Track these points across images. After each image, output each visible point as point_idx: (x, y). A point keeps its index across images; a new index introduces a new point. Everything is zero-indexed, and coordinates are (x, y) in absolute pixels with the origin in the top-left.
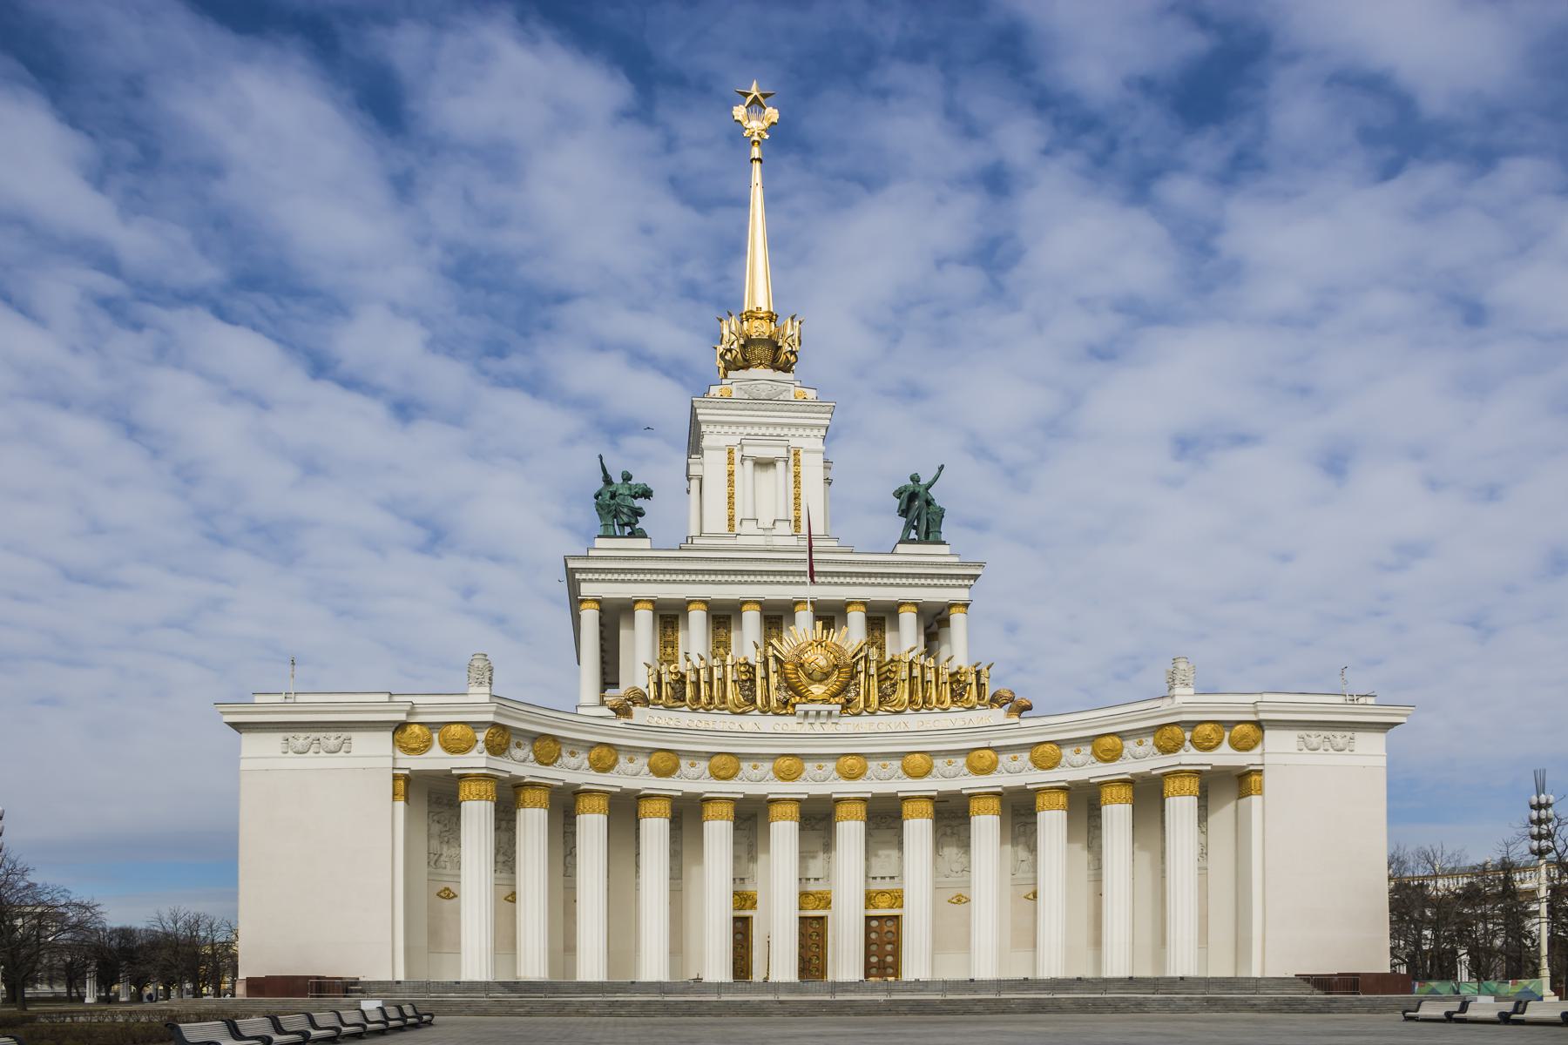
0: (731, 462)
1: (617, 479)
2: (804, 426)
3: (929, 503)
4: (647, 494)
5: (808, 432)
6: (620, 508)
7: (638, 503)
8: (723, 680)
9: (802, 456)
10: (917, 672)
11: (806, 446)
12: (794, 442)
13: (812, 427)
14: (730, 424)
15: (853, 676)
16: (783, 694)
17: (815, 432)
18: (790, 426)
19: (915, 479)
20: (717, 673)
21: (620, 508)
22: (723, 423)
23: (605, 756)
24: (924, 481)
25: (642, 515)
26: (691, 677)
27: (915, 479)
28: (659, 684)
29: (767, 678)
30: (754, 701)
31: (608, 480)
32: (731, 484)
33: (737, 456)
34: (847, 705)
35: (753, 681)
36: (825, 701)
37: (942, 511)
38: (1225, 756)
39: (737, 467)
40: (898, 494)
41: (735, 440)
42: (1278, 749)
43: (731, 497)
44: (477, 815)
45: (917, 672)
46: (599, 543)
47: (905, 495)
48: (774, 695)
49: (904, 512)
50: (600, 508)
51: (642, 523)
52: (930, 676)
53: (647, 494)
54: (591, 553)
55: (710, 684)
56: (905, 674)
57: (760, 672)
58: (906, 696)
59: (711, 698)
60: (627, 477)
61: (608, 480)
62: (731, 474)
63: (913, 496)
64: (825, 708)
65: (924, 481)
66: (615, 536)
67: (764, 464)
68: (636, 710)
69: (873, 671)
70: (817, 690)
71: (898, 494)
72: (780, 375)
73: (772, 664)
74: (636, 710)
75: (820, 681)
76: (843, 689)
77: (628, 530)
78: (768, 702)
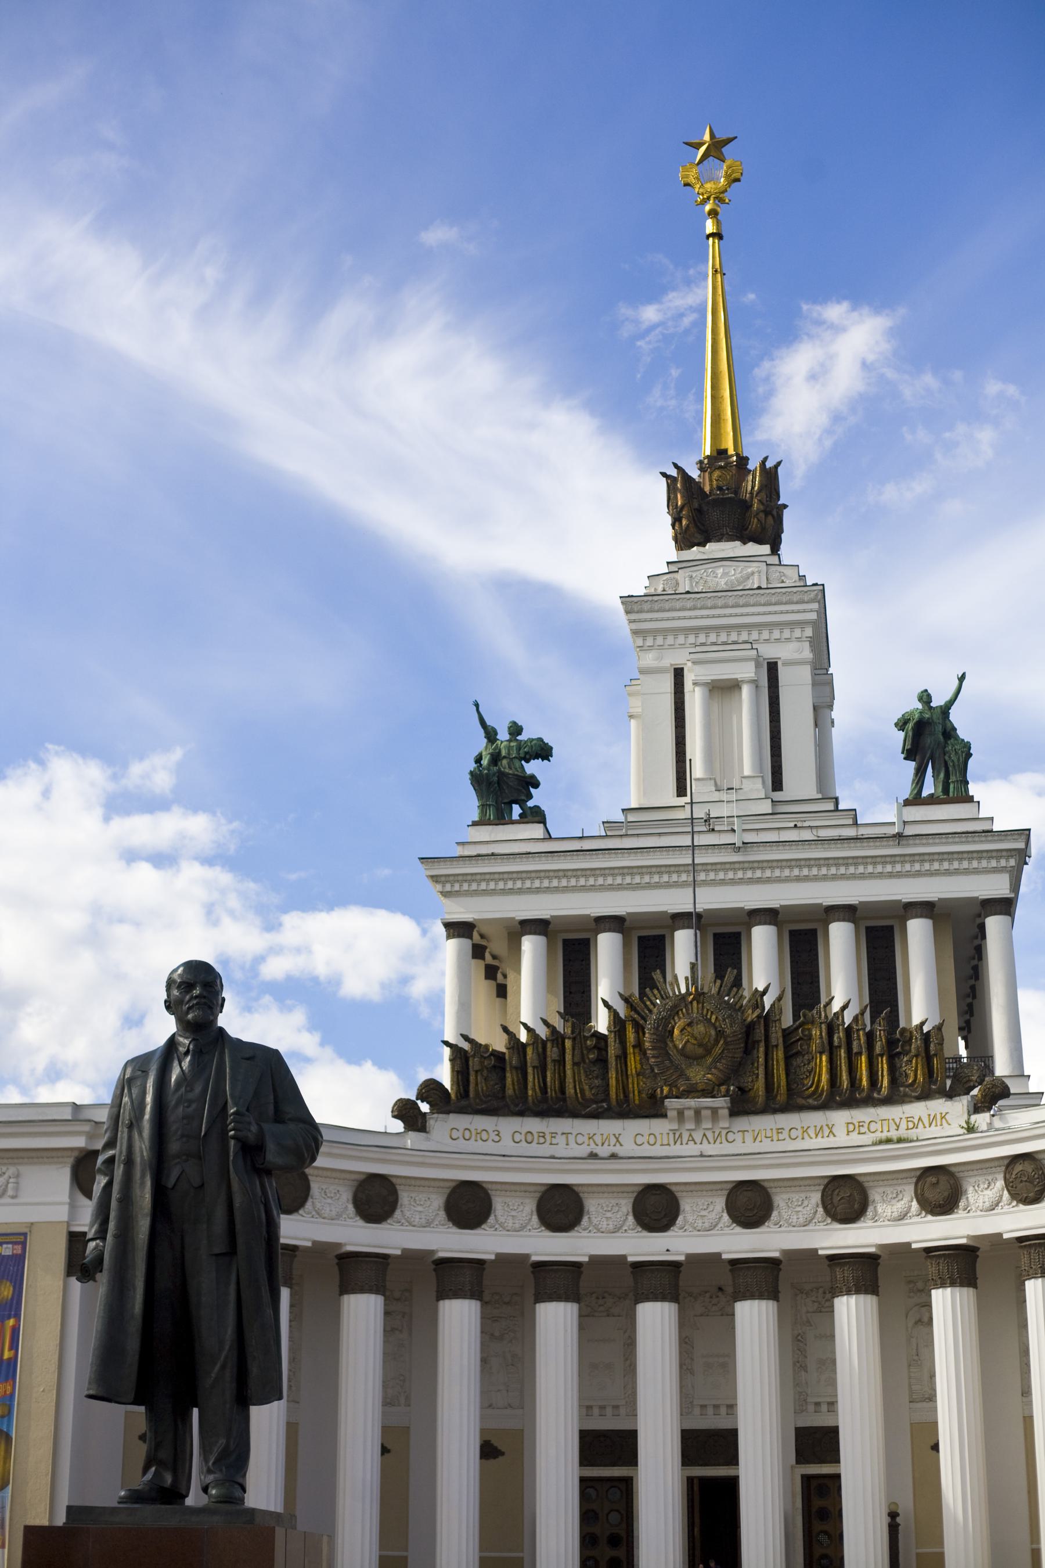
1: (503, 735)
2: (781, 625)
3: (949, 733)
4: (543, 751)
6: (505, 782)
7: (533, 767)
8: (561, 1062)
9: (783, 673)
10: (839, 1036)
12: (770, 652)
13: (792, 625)
14: (675, 631)
17: (797, 633)
18: (760, 626)
19: (925, 697)
20: (552, 1053)
21: (505, 782)
22: (665, 632)
23: (376, 1198)
24: (937, 702)
25: (536, 785)
27: (925, 697)
29: (623, 1057)
30: (607, 1098)
31: (491, 735)
33: (689, 679)
35: (602, 1061)
36: (709, 1092)
37: (968, 743)
40: (901, 724)
45: (839, 1036)
47: (910, 726)
48: (634, 1085)
49: (910, 754)
50: (478, 780)
51: (538, 798)
53: (543, 751)
55: (542, 1068)
57: (613, 1050)
58: (825, 1077)
59: (544, 1089)
60: (516, 730)
61: (491, 735)
64: (707, 1102)
65: (937, 702)
67: (723, 690)
70: (698, 1075)
71: (901, 724)
72: (752, 549)
73: (631, 1035)
75: (697, 1059)
77: (516, 810)
78: (626, 1096)
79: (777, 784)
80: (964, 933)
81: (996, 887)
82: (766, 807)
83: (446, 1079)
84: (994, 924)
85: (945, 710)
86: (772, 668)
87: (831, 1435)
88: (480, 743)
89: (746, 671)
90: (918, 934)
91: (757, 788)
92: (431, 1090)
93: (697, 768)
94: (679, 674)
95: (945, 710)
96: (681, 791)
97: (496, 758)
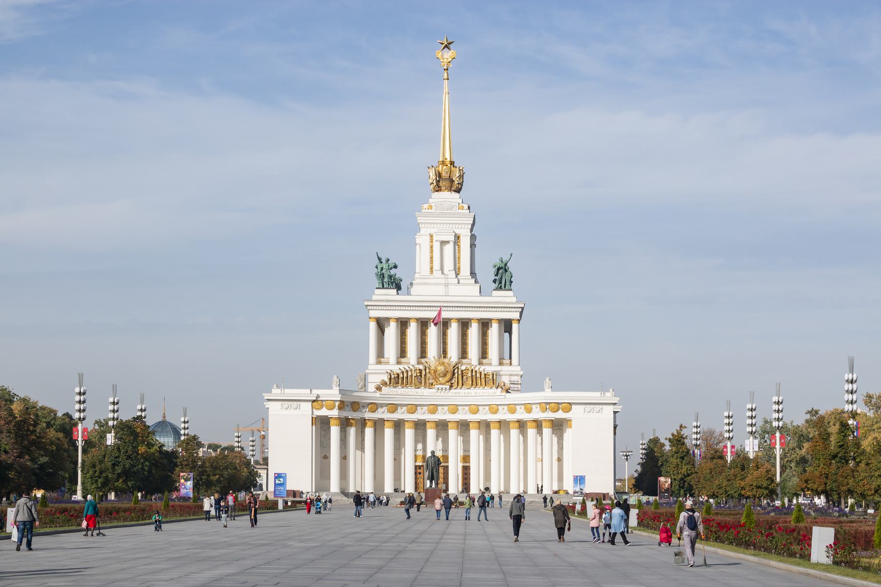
1: (384, 261)
7: (393, 271)
8: (411, 376)
9: (461, 238)
12: (458, 232)
15: (454, 374)
16: (431, 381)
20: (410, 374)
26: (401, 376)
28: (390, 379)
31: (380, 259)
32: (432, 252)
33: (435, 238)
35: (421, 376)
38: (560, 415)
41: (432, 231)
42: (575, 414)
44: (335, 431)
46: (378, 291)
52: (478, 375)
53: (395, 267)
54: (374, 297)
56: (470, 375)
57: (424, 373)
61: (380, 259)
63: (499, 269)
64: (444, 387)
66: (383, 287)
68: (383, 388)
73: (428, 371)
74: (383, 388)
76: (451, 379)
80: (507, 326)
81: (516, 315)
83: (387, 381)
84: (515, 326)
87: (469, 456)
88: (378, 261)
89: (452, 238)
92: (385, 384)
93: (436, 266)
94: (431, 236)
97: (382, 269)
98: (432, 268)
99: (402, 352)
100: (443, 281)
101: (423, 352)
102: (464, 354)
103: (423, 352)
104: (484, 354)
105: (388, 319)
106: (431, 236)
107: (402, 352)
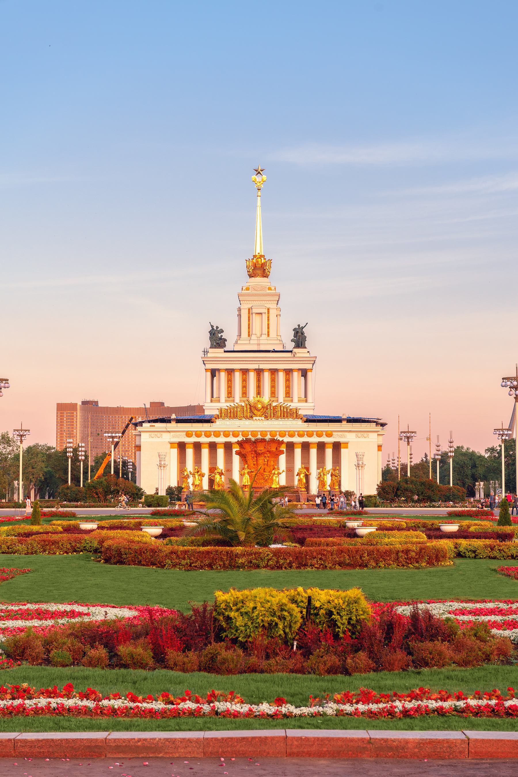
0: (249, 312)
3: (303, 333)
5: (272, 302)
9: (270, 310)
10: (282, 409)
11: (271, 307)
12: (268, 306)
17: (274, 302)
19: (299, 326)
21: (217, 339)
26: (229, 411)
27: (299, 326)
28: (221, 413)
31: (212, 326)
34: (266, 417)
39: (251, 315)
40: (294, 330)
41: (250, 306)
43: (249, 325)
45: (282, 409)
52: (285, 410)
57: (245, 409)
60: (217, 327)
61: (212, 326)
62: (249, 317)
63: (297, 332)
64: (260, 418)
66: (215, 347)
69: (272, 408)
71: (294, 330)
79: (268, 335)
82: (266, 342)
85: (303, 328)
86: (268, 309)
90: (295, 374)
91: (264, 337)
95: (303, 328)
96: (249, 336)
98: (249, 333)
99: (230, 394)
100: (256, 342)
101: (245, 393)
102: (273, 393)
103: (245, 393)
104: (288, 394)
105: (219, 370)
106: (249, 310)
107: (230, 394)
